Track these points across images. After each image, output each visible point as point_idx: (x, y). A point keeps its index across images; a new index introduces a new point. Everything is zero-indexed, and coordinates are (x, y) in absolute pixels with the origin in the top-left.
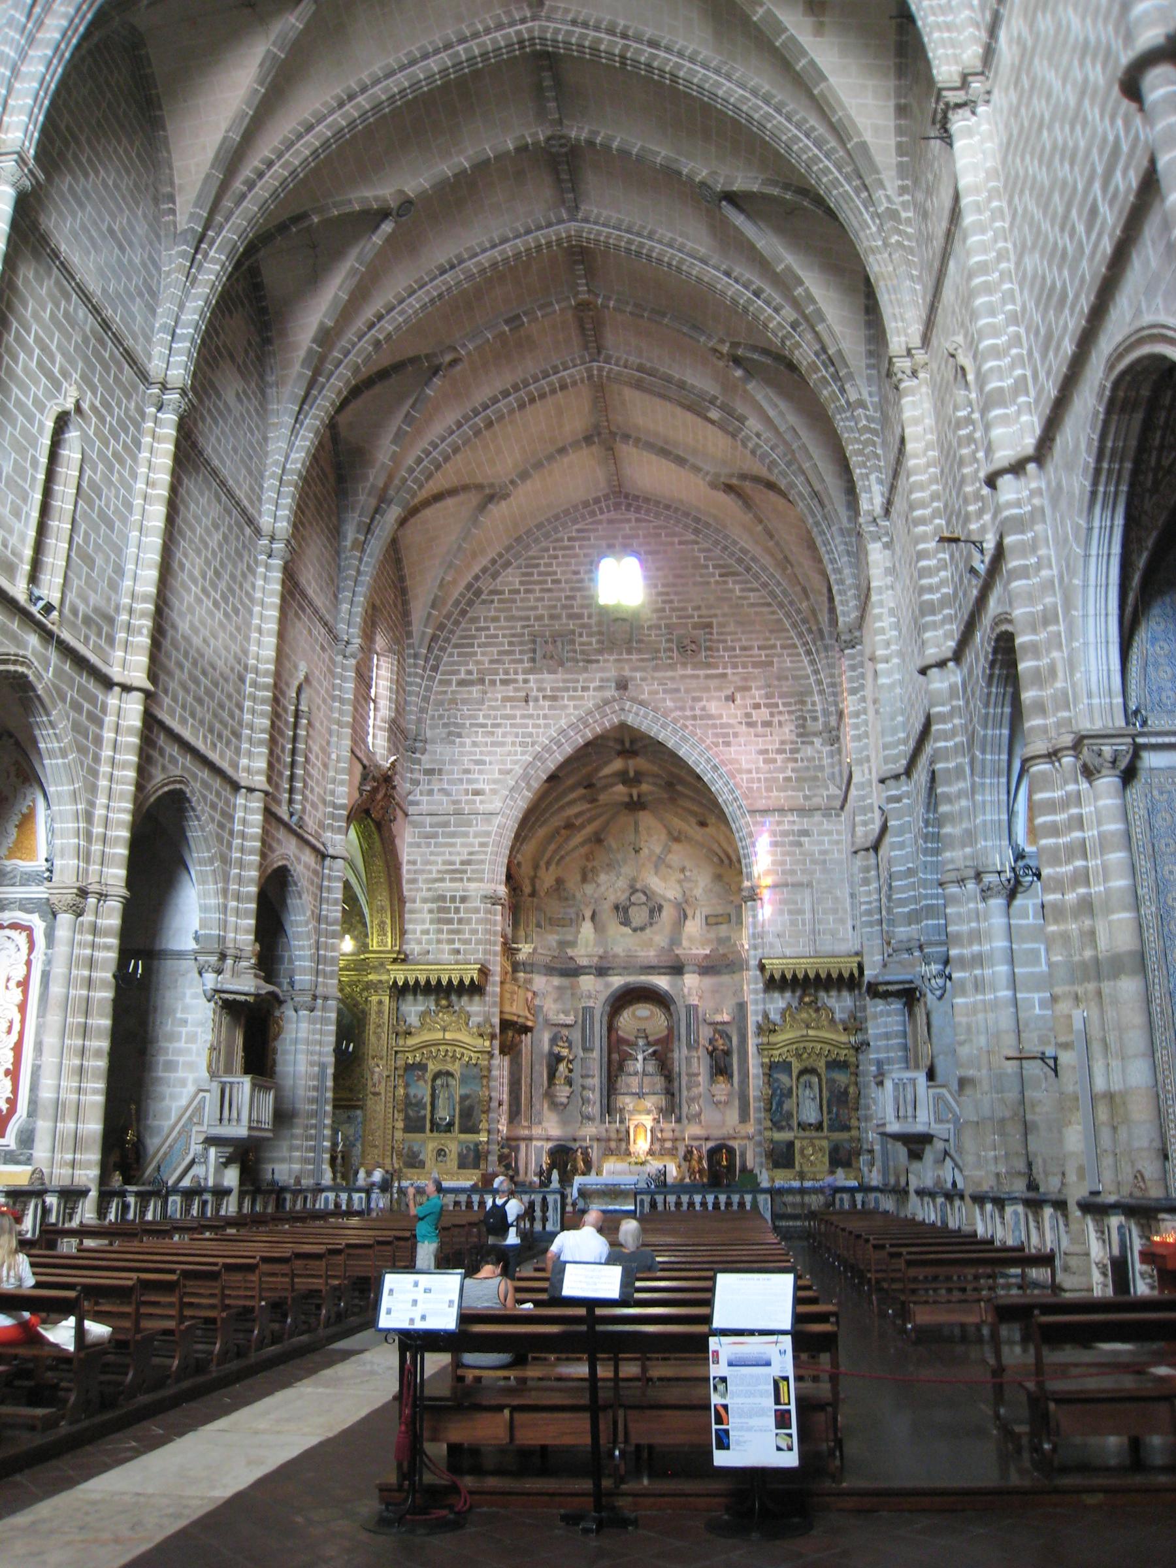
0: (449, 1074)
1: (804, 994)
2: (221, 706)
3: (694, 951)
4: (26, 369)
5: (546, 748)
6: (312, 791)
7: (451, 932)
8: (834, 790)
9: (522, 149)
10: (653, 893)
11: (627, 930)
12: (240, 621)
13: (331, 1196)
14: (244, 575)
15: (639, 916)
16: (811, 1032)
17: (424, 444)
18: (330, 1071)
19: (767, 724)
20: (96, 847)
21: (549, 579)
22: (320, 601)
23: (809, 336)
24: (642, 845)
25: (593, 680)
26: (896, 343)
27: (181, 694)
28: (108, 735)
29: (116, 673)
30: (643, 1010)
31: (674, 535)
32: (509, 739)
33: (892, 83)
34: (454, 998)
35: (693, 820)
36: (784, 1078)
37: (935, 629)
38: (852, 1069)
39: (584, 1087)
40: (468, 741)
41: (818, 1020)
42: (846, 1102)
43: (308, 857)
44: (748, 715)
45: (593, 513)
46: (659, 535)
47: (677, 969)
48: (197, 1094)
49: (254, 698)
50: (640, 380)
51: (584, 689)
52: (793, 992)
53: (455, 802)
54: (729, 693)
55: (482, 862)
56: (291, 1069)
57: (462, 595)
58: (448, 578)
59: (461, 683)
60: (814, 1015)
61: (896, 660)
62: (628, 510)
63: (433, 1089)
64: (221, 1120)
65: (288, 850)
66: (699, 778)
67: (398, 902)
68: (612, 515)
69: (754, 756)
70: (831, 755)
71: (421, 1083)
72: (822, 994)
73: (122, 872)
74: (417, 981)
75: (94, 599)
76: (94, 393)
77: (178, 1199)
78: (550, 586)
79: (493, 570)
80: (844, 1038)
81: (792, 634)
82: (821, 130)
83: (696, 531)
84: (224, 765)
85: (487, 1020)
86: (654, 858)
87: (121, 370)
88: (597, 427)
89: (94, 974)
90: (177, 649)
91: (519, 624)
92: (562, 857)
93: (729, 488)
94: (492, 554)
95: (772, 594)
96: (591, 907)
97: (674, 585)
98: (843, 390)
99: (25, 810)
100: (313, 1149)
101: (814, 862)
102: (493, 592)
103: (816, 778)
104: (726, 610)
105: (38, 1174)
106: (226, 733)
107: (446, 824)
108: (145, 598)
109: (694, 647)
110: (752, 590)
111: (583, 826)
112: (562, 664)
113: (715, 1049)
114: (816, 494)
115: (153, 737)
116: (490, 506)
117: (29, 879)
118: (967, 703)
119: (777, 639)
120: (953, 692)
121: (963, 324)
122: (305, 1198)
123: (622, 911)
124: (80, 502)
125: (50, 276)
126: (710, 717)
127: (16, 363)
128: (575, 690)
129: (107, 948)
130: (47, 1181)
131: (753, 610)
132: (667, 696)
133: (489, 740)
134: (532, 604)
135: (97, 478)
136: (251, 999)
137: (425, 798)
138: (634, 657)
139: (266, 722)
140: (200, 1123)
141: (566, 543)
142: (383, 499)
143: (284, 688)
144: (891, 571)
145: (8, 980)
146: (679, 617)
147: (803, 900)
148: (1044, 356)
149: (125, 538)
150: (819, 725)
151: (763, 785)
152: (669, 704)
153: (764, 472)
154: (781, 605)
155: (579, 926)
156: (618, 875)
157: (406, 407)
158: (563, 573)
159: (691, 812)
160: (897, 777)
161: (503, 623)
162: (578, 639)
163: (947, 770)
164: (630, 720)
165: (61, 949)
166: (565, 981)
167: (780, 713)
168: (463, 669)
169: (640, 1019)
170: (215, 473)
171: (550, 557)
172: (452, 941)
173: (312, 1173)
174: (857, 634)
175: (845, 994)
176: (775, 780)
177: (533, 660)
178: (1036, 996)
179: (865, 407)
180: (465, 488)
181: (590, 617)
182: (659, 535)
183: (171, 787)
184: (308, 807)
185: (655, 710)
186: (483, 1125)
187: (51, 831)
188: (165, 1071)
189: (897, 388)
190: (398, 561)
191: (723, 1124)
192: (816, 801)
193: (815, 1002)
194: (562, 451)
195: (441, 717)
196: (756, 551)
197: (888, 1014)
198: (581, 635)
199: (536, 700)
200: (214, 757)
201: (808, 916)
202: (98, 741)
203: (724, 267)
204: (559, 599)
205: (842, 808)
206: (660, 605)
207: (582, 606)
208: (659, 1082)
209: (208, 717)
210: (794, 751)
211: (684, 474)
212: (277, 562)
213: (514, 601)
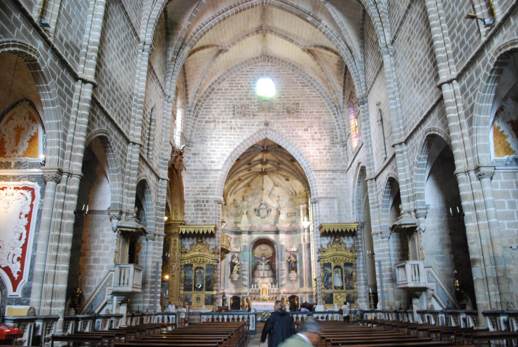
0: (201, 268)
1: (335, 238)
3: (283, 225)
5: (239, 146)
7: (202, 214)
8: (344, 164)
10: (268, 205)
11: (259, 218)
12: (131, 73)
13: (160, 317)
15: (263, 213)
16: (338, 252)
17: (199, 24)
18: (161, 265)
19: (320, 139)
20: (67, 152)
21: (239, 85)
22: (160, 78)
24: (265, 187)
25: (256, 122)
27: (107, 95)
28: (75, 101)
29: (80, 74)
30: (263, 247)
31: (285, 71)
32: (225, 143)
34: (204, 239)
35: (284, 179)
36: (328, 269)
38: (354, 266)
40: (209, 143)
41: (341, 248)
42: (352, 279)
44: (313, 136)
45: (255, 63)
46: (280, 71)
48: (109, 273)
50: (282, 5)
52: (331, 237)
53: (204, 166)
54: (306, 128)
55: (214, 188)
56: (144, 264)
57: (207, 90)
58: (203, 82)
59: (207, 122)
60: (339, 246)
61: (398, 99)
62: (268, 62)
63: (195, 274)
64: (120, 284)
65: (146, 173)
67: (182, 201)
68: (262, 63)
69: (315, 151)
70: (343, 151)
71: (190, 272)
72: (342, 238)
73: (80, 164)
74: (190, 232)
77: (100, 320)
78: (239, 88)
79: (218, 82)
80: (350, 254)
81: (328, 107)
83: (293, 70)
84: (124, 131)
85: (216, 247)
86: (268, 193)
88: (261, 27)
89: (65, 212)
90: (106, 75)
91: (228, 101)
92: (236, 192)
93: (309, 51)
94: (218, 75)
97: (285, 89)
99: (33, 134)
100: (152, 297)
102: (218, 89)
103: (338, 159)
104: (304, 98)
105: (32, 310)
106: (125, 118)
107: (201, 174)
108: (94, 44)
109: (293, 111)
110: (314, 92)
111: (244, 180)
112: (244, 116)
113: (291, 261)
114: (349, 48)
115: (95, 110)
116: (220, 55)
117: (33, 165)
119: (323, 109)
122: (151, 318)
123: (257, 211)
126: (299, 136)
128: (249, 125)
129: (72, 199)
130: (37, 314)
131: (314, 99)
132: (283, 129)
133: (217, 143)
134: (233, 94)
136: (134, 230)
137: (193, 164)
138: (271, 114)
139: (141, 117)
140: (110, 286)
141: (245, 73)
142: (184, 44)
143: (147, 107)
145: (21, 214)
146: (287, 100)
147: (334, 203)
150: (339, 140)
151: (318, 161)
152: (284, 131)
153: (326, 42)
154: (324, 97)
156: (256, 199)
157: (194, 7)
158: (244, 83)
159: (284, 176)
160: (400, 144)
161: (222, 101)
162: (250, 107)
164: (269, 137)
165: (48, 198)
166: (237, 236)
167: (324, 135)
168: (207, 117)
169: (262, 250)
170: (123, 7)
171: (240, 77)
172: (203, 217)
173: (152, 308)
174: (365, 99)
175: (350, 238)
177: (234, 114)
178: (505, 222)
179: (382, 4)
180: (212, 46)
181: (254, 99)
182: (280, 71)
184: (154, 158)
185: (279, 133)
186: (215, 288)
187: (45, 144)
188: (94, 263)
190: (185, 74)
191: (293, 288)
192: (338, 168)
193: (339, 241)
194: (247, 35)
195: (199, 134)
196: (316, 78)
197: (383, 242)
198: (251, 106)
199: (235, 129)
200: (120, 126)
201: (336, 209)
202: (70, 103)
204: (243, 93)
205: (348, 170)
206: (280, 96)
207: (251, 96)
208: (270, 273)
209: (118, 109)
211: (292, 46)
212: (146, 54)
213: (227, 93)
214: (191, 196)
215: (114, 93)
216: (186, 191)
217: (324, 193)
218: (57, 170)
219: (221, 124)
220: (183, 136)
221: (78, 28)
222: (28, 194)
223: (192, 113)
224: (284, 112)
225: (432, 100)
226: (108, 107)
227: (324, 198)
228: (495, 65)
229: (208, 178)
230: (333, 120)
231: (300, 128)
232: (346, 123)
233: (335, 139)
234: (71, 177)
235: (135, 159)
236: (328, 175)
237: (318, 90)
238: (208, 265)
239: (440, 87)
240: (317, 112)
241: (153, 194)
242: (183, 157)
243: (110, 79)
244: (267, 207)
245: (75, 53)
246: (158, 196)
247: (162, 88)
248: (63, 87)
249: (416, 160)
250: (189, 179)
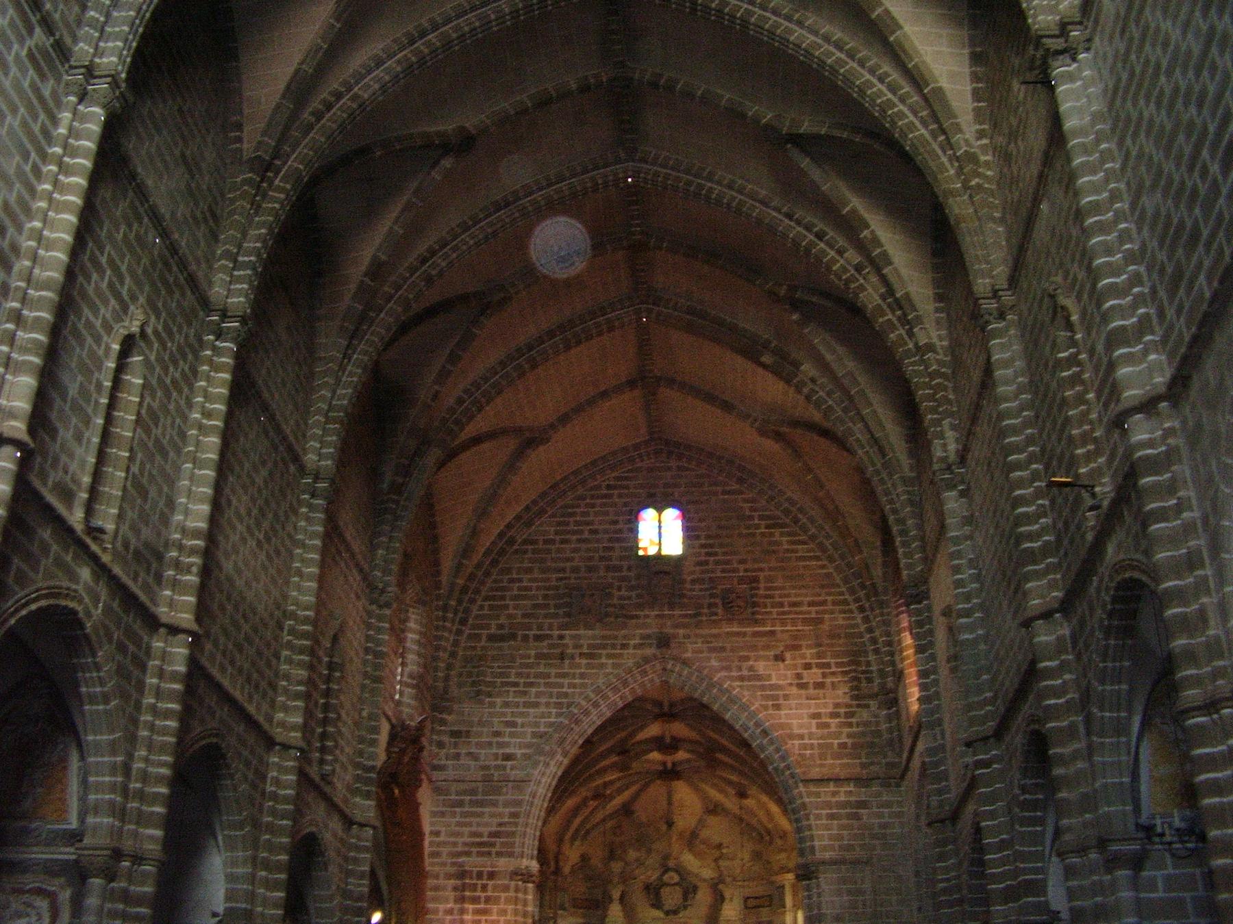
2: (259, 653)
4: (97, 288)
6: (342, 751)
8: (891, 758)
11: (658, 913)
14: (287, 517)
15: (671, 897)
22: (356, 546)
23: (874, 279)
26: (982, 285)
27: (222, 640)
29: (162, 611)
31: (715, 484)
32: (543, 700)
33: (965, 33)
37: (1038, 579)
43: (336, 824)
44: (799, 676)
45: (631, 460)
49: (289, 646)
51: (624, 646)
55: (513, 834)
59: (491, 638)
66: (746, 744)
70: (889, 719)
75: (146, 533)
76: (158, 318)
78: (586, 535)
79: (527, 517)
82: (895, 76)
83: (740, 481)
87: (183, 294)
90: (222, 591)
92: (588, 832)
95: (821, 546)
96: (621, 887)
98: (911, 334)
101: (874, 837)
102: (525, 542)
106: (263, 684)
107: (473, 792)
108: (196, 534)
111: (612, 797)
114: (875, 441)
118: (1079, 657)
119: (829, 594)
120: (1060, 643)
121: (1061, 264)
123: (654, 893)
124: (139, 430)
125: (125, 197)
126: (759, 678)
127: (89, 282)
128: (614, 646)
134: (568, 555)
135: (156, 405)
138: (677, 612)
144: (969, 520)
146: (723, 571)
148: (1173, 291)
149: (178, 469)
152: (714, 663)
154: (831, 559)
155: (606, 909)
156: (649, 851)
159: (730, 783)
161: (536, 575)
163: (1060, 729)
167: (833, 674)
168: (493, 623)
170: (265, 408)
171: (587, 505)
176: (830, 745)
179: (935, 352)
180: (504, 432)
181: (629, 569)
182: (702, 485)
184: (338, 770)
187: (84, 783)
189: (983, 330)
194: (604, 395)
195: (470, 675)
198: (619, 589)
199: (573, 657)
200: (251, 709)
202: (141, 686)
203: (785, 209)
204: (596, 550)
205: (902, 777)
207: (621, 558)
209: (246, 666)
210: (850, 715)
213: (549, 551)
214: (444, 858)
215: (239, 628)
216: (431, 843)
217: (832, 848)
218: (108, 852)
219: (532, 643)
220: (421, 684)
222: (43, 904)
223: (450, 615)
224: (716, 605)
227: (834, 862)
228: (1115, 600)
230: (856, 626)
231: (761, 653)
233: (864, 684)
234: (140, 865)
235: (285, 788)
236: (845, 793)
237: (813, 538)
240: (810, 604)
241: (333, 869)
242: (421, 749)
244: (682, 878)
247: (361, 571)
249: (1017, 791)
250: (440, 809)
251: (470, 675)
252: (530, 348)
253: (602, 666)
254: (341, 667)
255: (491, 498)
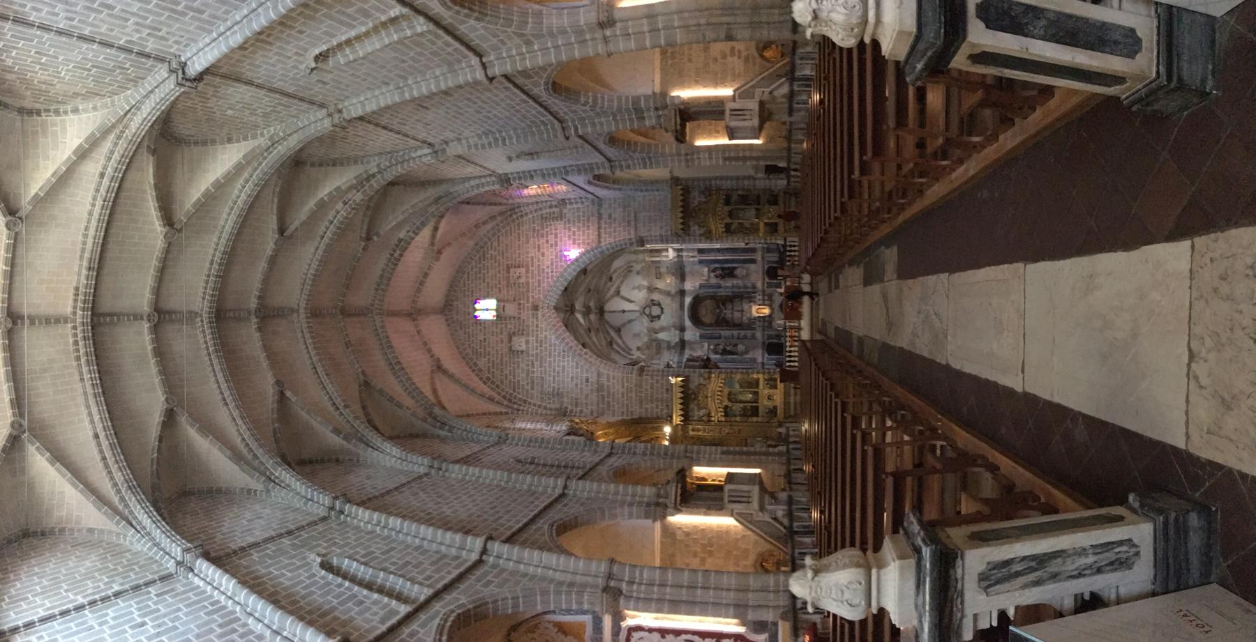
0: (729, 394)
9: (260, 329)
11: (663, 317)
22: (477, 448)
29: (474, 557)
36: (733, 227)
39: (738, 338)
43: (612, 460)
44: (552, 245)
47: (682, 293)
51: (537, 326)
59: (532, 389)
61: (504, 134)
68: (454, 312)
70: (571, 203)
77: (795, 524)
79: (478, 372)
83: (464, 273)
85: (701, 375)
93: (439, 252)
106: (531, 499)
111: (612, 338)
136: (680, 486)
154: (499, 231)
166: (687, 347)
168: (526, 387)
180: (432, 378)
183: (554, 531)
186: (755, 376)
194: (419, 332)
195: (549, 399)
202: (513, 573)
208: (737, 301)
217: (629, 231)
221: (415, 554)
225: (507, 89)
226: (518, 522)
227: (636, 229)
229: (608, 386)
232: (534, 200)
237: (490, 239)
238: (724, 384)
239: (491, 79)
243: (478, 516)
245: (446, 560)
246: (635, 453)
248: (492, 582)
249: (587, 108)
251: (549, 399)
252: (390, 364)
253: (546, 337)
254: (533, 458)
255: (466, 387)
